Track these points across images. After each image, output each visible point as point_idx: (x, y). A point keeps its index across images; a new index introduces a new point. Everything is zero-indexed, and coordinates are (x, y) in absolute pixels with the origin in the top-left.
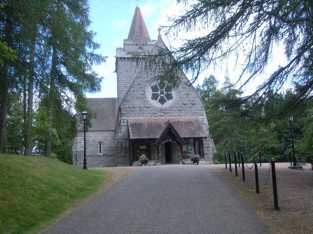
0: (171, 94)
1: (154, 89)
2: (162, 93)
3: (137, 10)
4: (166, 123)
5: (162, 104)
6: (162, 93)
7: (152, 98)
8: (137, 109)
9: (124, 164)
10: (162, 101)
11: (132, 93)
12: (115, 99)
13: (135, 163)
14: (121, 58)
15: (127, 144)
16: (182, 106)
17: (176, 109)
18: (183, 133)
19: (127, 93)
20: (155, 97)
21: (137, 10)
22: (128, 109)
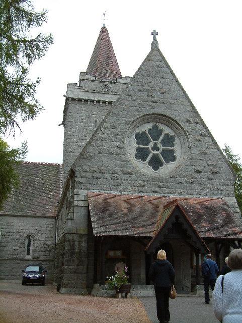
0: (173, 152)
1: (141, 138)
2: (155, 148)
3: (104, 32)
4: (166, 207)
5: (156, 168)
6: (155, 148)
8: (107, 176)
9: (73, 289)
10: (156, 163)
11: (99, 142)
12: (57, 166)
14: (73, 99)
15: (84, 244)
16: (196, 175)
17: (182, 180)
18: (204, 230)
19: (89, 143)
20: (141, 154)
21: (104, 32)
22: (89, 175)
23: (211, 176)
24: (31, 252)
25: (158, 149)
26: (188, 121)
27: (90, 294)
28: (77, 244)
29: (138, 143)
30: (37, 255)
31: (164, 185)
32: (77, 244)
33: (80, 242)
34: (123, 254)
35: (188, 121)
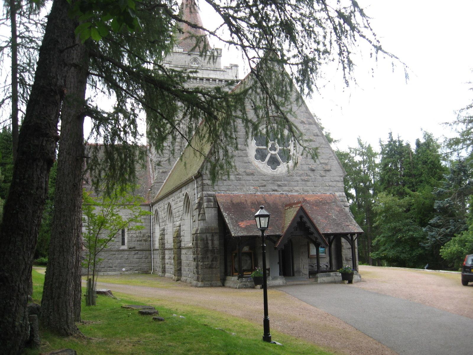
7: (256, 157)
10: (274, 162)
13: (233, 280)
15: (216, 242)
16: (311, 174)
17: (298, 178)
23: (323, 173)
24: (126, 241)
25: (275, 150)
26: (302, 122)
27: (223, 285)
28: (210, 242)
29: (257, 144)
30: (132, 245)
31: (283, 184)
32: (210, 242)
33: (212, 240)
34: (250, 249)
35: (302, 122)
